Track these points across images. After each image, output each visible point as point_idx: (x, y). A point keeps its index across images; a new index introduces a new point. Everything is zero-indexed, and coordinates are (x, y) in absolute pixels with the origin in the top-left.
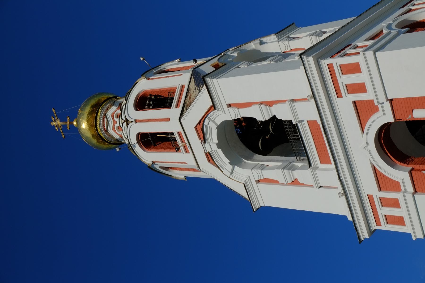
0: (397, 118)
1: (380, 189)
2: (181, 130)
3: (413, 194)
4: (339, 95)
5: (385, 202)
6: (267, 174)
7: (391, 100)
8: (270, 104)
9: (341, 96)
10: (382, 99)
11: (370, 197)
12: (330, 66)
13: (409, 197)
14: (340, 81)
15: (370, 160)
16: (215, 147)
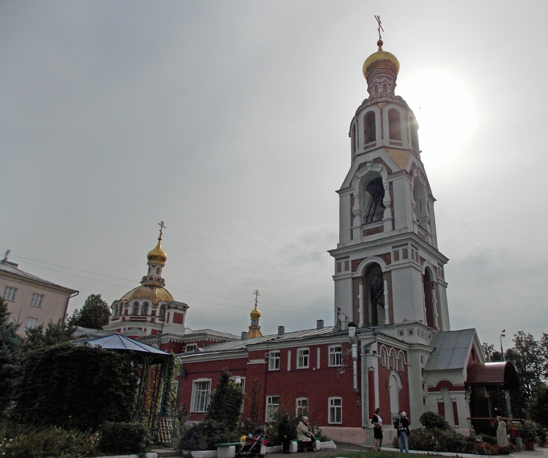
0: (383, 274)
1: (352, 261)
2: (377, 146)
3: (352, 277)
4: (393, 247)
5: (347, 264)
6: (356, 201)
7: (390, 272)
8: (392, 206)
9: (393, 248)
10: (391, 268)
11: (348, 257)
12: (407, 244)
13: (350, 276)
14: (400, 248)
15: (366, 258)
16: (369, 169)
